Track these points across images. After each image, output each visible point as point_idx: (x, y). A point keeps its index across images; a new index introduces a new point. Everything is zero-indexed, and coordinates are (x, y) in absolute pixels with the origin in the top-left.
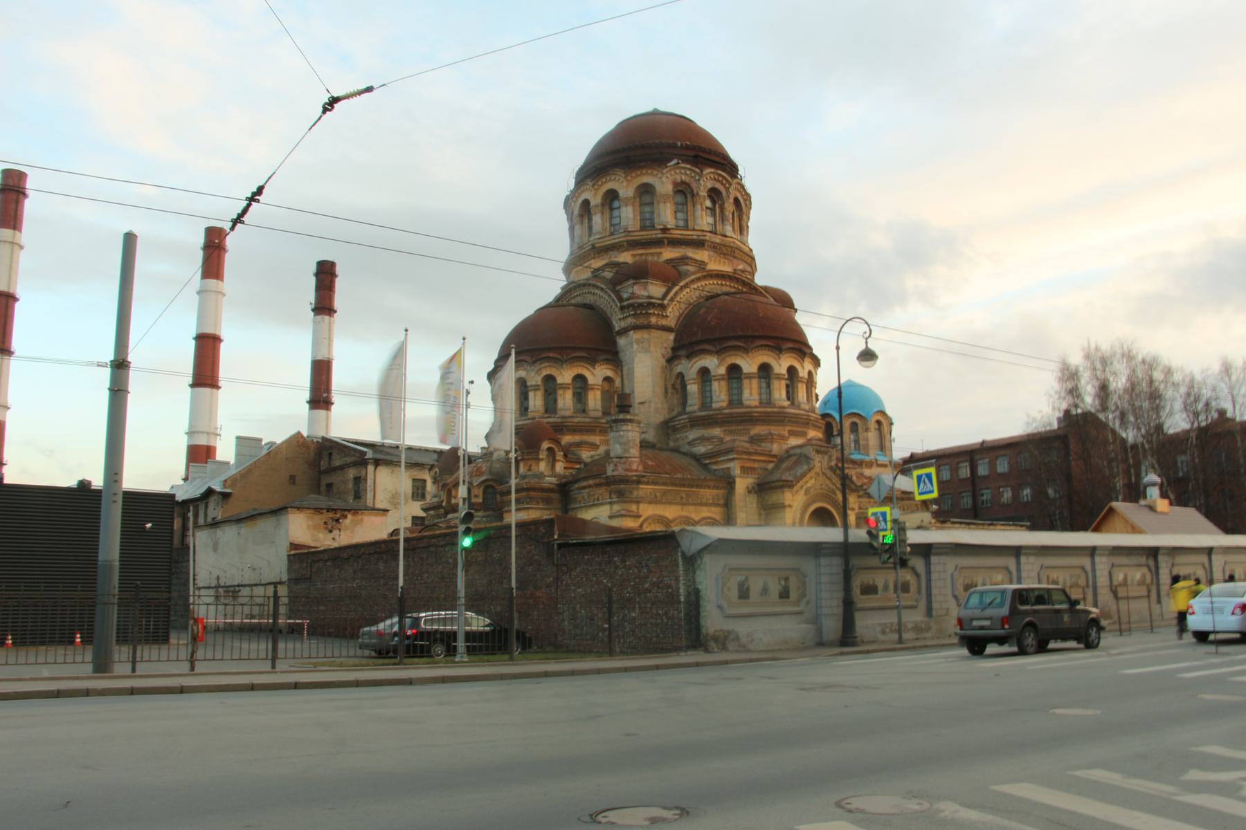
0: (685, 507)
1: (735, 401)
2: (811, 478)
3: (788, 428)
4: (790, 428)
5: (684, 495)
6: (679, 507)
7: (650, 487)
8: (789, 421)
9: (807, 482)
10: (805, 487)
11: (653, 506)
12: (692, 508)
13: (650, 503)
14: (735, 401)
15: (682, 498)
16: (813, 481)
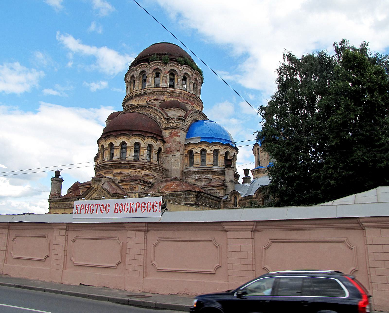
0: (66, 210)
1: (137, 159)
2: (94, 193)
3: (104, 171)
4: (105, 171)
5: (65, 205)
6: (64, 210)
7: (54, 203)
8: (104, 168)
9: (92, 195)
10: (91, 197)
11: (55, 210)
12: (68, 210)
13: (54, 209)
14: (137, 159)
15: (65, 206)
16: (95, 194)
